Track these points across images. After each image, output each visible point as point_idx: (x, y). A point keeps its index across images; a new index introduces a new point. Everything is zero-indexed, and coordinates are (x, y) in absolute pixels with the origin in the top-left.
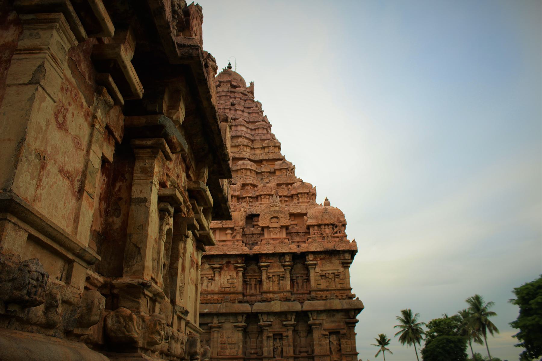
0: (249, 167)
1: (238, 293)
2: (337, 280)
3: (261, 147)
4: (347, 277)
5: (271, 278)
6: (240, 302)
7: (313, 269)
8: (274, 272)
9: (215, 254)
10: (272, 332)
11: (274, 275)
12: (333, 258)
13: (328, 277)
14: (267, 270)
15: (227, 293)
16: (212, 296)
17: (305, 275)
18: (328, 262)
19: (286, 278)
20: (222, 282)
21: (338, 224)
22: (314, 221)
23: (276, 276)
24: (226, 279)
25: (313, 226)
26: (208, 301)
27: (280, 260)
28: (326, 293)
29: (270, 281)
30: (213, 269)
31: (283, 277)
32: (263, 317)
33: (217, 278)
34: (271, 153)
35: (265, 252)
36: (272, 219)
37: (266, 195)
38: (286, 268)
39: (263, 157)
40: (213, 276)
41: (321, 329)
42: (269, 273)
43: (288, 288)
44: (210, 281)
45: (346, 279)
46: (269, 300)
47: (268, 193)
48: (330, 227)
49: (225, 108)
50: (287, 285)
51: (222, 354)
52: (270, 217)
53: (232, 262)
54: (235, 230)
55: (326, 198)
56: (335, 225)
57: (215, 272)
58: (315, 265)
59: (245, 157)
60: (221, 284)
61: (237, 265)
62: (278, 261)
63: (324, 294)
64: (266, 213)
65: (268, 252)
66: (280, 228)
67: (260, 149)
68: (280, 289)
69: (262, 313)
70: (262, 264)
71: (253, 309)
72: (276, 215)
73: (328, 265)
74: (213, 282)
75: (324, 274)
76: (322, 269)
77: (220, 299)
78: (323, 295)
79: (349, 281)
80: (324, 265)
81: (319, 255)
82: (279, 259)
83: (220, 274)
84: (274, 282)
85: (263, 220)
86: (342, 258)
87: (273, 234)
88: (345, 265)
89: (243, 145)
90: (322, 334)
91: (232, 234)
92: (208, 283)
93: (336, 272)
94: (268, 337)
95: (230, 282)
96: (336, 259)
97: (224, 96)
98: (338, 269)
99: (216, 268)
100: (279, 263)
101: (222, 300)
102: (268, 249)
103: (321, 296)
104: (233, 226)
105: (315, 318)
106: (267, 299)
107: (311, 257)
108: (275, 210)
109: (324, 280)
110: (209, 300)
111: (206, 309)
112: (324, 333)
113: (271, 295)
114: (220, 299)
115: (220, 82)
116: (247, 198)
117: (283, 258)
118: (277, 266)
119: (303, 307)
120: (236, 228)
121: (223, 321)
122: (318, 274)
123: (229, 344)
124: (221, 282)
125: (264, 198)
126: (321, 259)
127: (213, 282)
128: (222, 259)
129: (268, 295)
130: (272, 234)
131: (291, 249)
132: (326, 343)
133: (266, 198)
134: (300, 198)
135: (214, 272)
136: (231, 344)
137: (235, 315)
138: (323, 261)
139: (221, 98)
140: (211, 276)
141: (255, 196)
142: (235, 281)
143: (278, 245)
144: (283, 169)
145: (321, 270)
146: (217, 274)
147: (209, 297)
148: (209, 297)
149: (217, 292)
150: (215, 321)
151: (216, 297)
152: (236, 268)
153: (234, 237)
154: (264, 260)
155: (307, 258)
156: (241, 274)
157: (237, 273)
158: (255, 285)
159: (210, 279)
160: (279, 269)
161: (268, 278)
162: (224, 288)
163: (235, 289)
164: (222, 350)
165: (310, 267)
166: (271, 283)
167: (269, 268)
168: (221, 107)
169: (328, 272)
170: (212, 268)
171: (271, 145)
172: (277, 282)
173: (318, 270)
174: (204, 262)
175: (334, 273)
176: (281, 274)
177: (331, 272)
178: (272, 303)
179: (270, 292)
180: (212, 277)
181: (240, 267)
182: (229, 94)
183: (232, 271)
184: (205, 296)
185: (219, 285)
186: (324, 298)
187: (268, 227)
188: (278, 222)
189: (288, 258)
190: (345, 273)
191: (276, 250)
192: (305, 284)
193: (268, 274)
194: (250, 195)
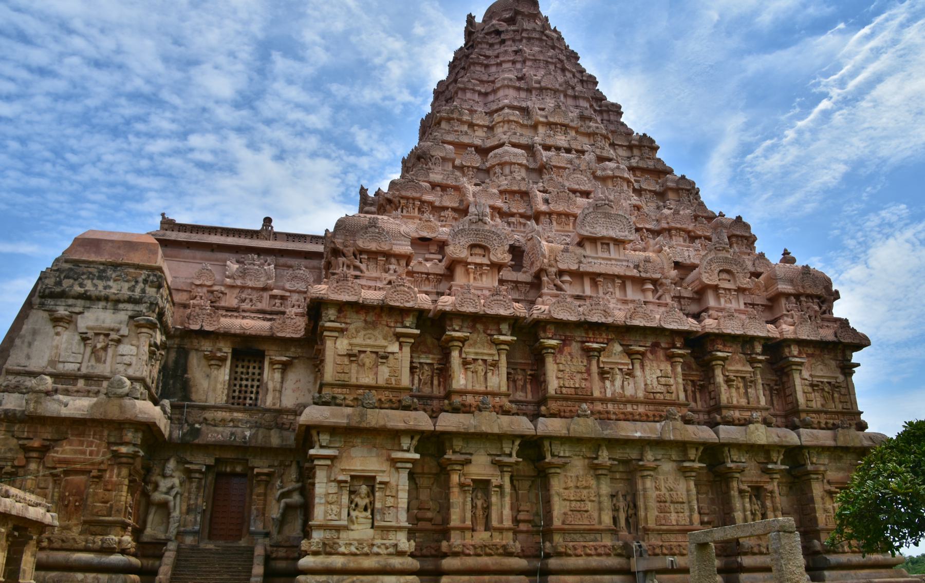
0: (626, 175)
1: (680, 405)
2: (836, 395)
3: (626, 144)
4: (848, 392)
5: (733, 381)
6: (687, 421)
7: (798, 372)
8: (738, 371)
9: (642, 325)
10: (748, 482)
11: (737, 377)
12: (826, 356)
13: (823, 390)
14: (723, 366)
15: (661, 404)
16: (635, 407)
17: (774, 382)
18: (819, 363)
19: (755, 385)
20: (649, 382)
21: (828, 297)
22: (789, 287)
23: (739, 379)
24: (654, 376)
25: (787, 296)
26: (630, 417)
27: (742, 349)
28: (823, 416)
29: (730, 386)
30: (630, 354)
31: (751, 382)
32: (732, 453)
33: (638, 373)
34: (648, 158)
35: (729, 331)
36: (721, 274)
37: (680, 229)
38: (756, 365)
39: (637, 163)
40: (631, 367)
41: (823, 481)
42: (728, 371)
43: (763, 402)
44: (627, 377)
45: (850, 394)
46: (737, 422)
47: (684, 226)
48: (815, 300)
49: (547, 62)
50: (761, 399)
51: (663, 522)
52: (718, 269)
53: (663, 345)
54: (662, 284)
55: (785, 250)
56: (822, 299)
57: (635, 361)
58: (801, 364)
59: (611, 156)
60: (646, 385)
61: (676, 350)
62: (740, 350)
63: (823, 419)
64: (711, 260)
65: (733, 333)
66: (735, 290)
67: (624, 148)
68: (748, 403)
69: (732, 446)
70: (719, 354)
71: (721, 436)
72: (727, 267)
73: (820, 367)
74: (631, 380)
75: (815, 383)
76: (813, 373)
77: (650, 414)
78: (821, 421)
79: (855, 398)
80: (813, 366)
81: (806, 349)
82: (742, 347)
83: (643, 366)
84: (738, 388)
85: (708, 273)
86: (840, 358)
87: (726, 301)
88: (847, 371)
89: (602, 135)
90: (826, 491)
91: (653, 291)
92: (623, 381)
93: (833, 381)
94: (741, 492)
95: (663, 383)
96: (831, 359)
97: (537, 39)
98: (836, 375)
99: (638, 353)
100: (742, 355)
101: (654, 415)
102: (732, 328)
103: (819, 422)
104: (658, 276)
105: (814, 460)
106: (734, 420)
107: (795, 350)
108: (726, 258)
109: (816, 394)
110: (632, 414)
111: (636, 432)
112: (828, 487)
113: (737, 414)
114: (650, 414)
115: (517, 13)
116: (645, 231)
117: (748, 346)
118: (740, 361)
119: (802, 439)
120: (664, 281)
121: (659, 457)
122: (807, 382)
123: (672, 502)
124: (645, 381)
125: (676, 236)
126: (808, 356)
127: (631, 379)
128: (645, 337)
129: (732, 412)
130: (722, 300)
131: (769, 331)
132: (833, 507)
133: (680, 236)
134: (735, 245)
135: (632, 360)
136: (677, 503)
137: (683, 446)
138: (813, 361)
139: (532, 41)
140: (626, 367)
141: (657, 228)
142: (672, 381)
143: (748, 321)
144: (682, 189)
145: (811, 375)
146: (637, 366)
147: (629, 408)
148: (629, 408)
149: (642, 399)
150: (649, 456)
151: (641, 409)
152: (670, 358)
153: (659, 298)
154: (720, 347)
155: (787, 350)
156: (679, 369)
157: (673, 365)
158: (694, 392)
159: (627, 374)
160: (744, 365)
161: (728, 381)
162: (653, 393)
163: (674, 396)
164: (662, 515)
165: (794, 367)
166: (733, 390)
167: (727, 362)
168: (541, 58)
169: (822, 380)
170: (627, 353)
171: (645, 144)
172: (742, 390)
173: (806, 374)
174: (611, 339)
175: (829, 383)
176: (748, 375)
177: (825, 380)
178: (751, 426)
179: (735, 408)
180: (628, 369)
181: (680, 356)
182: (544, 38)
183: (662, 361)
184: (622, 406)
185: (643, 386)
186: (823, 425)
187: (716, 288)
188: (729, 281)
189: (759, 349)
190: (848, 385)
191: (746, 330)
192: (774, 397)
193: (727, 374)
194: (648, 226)
